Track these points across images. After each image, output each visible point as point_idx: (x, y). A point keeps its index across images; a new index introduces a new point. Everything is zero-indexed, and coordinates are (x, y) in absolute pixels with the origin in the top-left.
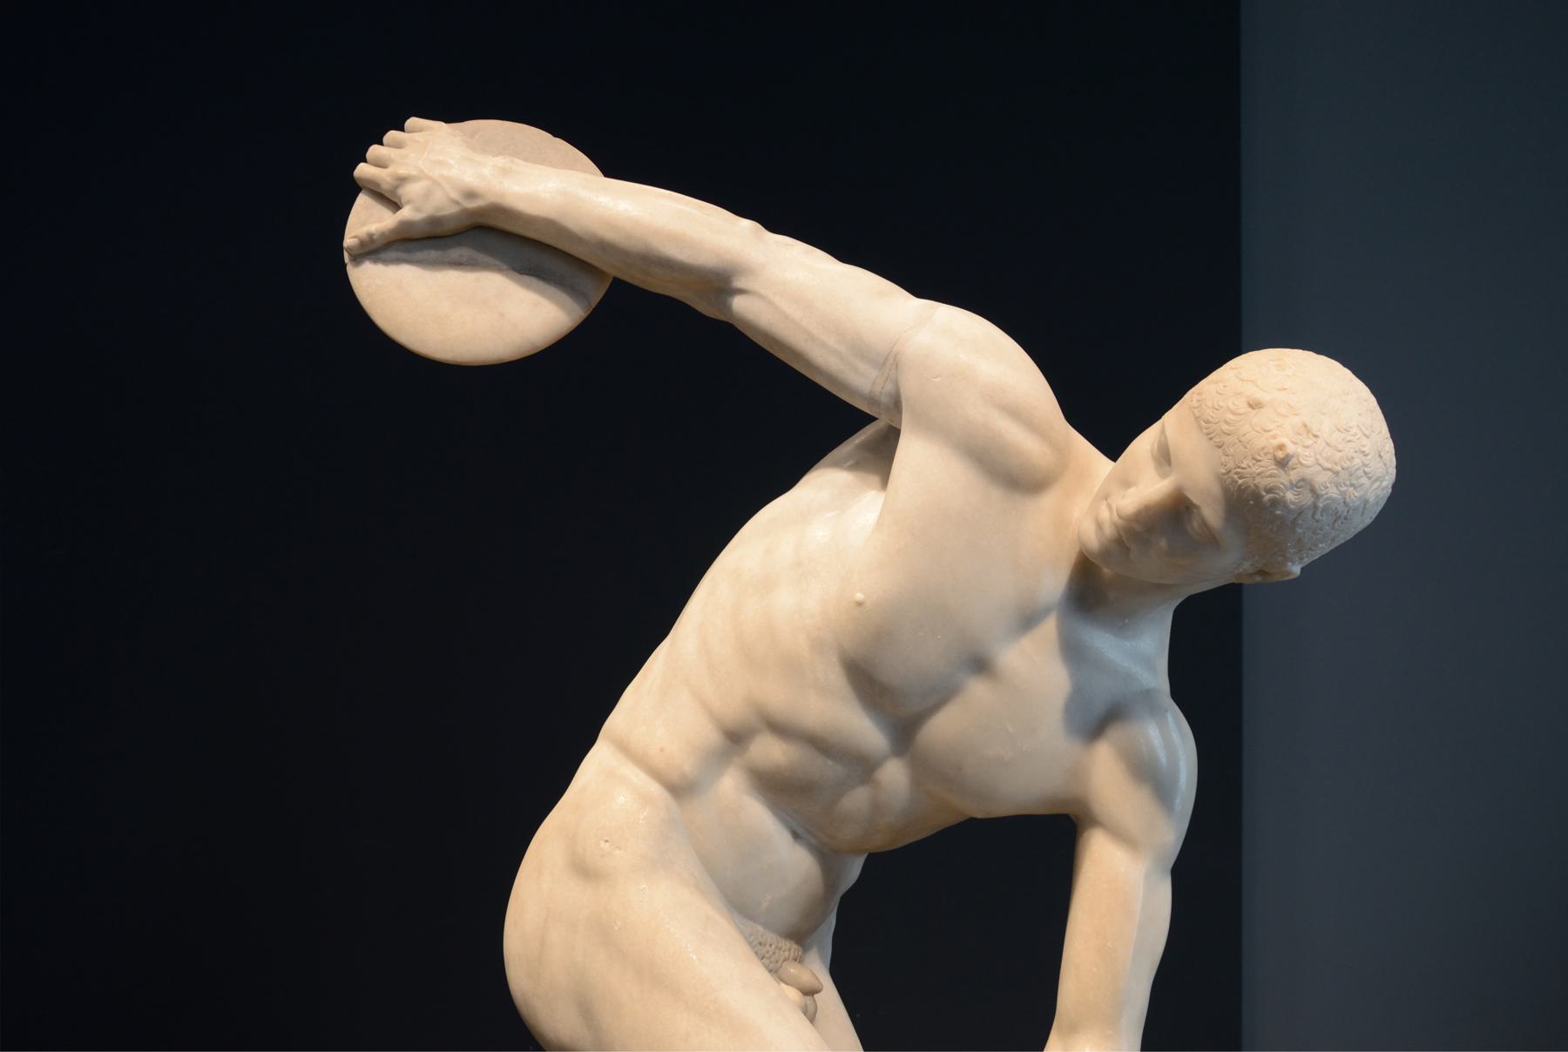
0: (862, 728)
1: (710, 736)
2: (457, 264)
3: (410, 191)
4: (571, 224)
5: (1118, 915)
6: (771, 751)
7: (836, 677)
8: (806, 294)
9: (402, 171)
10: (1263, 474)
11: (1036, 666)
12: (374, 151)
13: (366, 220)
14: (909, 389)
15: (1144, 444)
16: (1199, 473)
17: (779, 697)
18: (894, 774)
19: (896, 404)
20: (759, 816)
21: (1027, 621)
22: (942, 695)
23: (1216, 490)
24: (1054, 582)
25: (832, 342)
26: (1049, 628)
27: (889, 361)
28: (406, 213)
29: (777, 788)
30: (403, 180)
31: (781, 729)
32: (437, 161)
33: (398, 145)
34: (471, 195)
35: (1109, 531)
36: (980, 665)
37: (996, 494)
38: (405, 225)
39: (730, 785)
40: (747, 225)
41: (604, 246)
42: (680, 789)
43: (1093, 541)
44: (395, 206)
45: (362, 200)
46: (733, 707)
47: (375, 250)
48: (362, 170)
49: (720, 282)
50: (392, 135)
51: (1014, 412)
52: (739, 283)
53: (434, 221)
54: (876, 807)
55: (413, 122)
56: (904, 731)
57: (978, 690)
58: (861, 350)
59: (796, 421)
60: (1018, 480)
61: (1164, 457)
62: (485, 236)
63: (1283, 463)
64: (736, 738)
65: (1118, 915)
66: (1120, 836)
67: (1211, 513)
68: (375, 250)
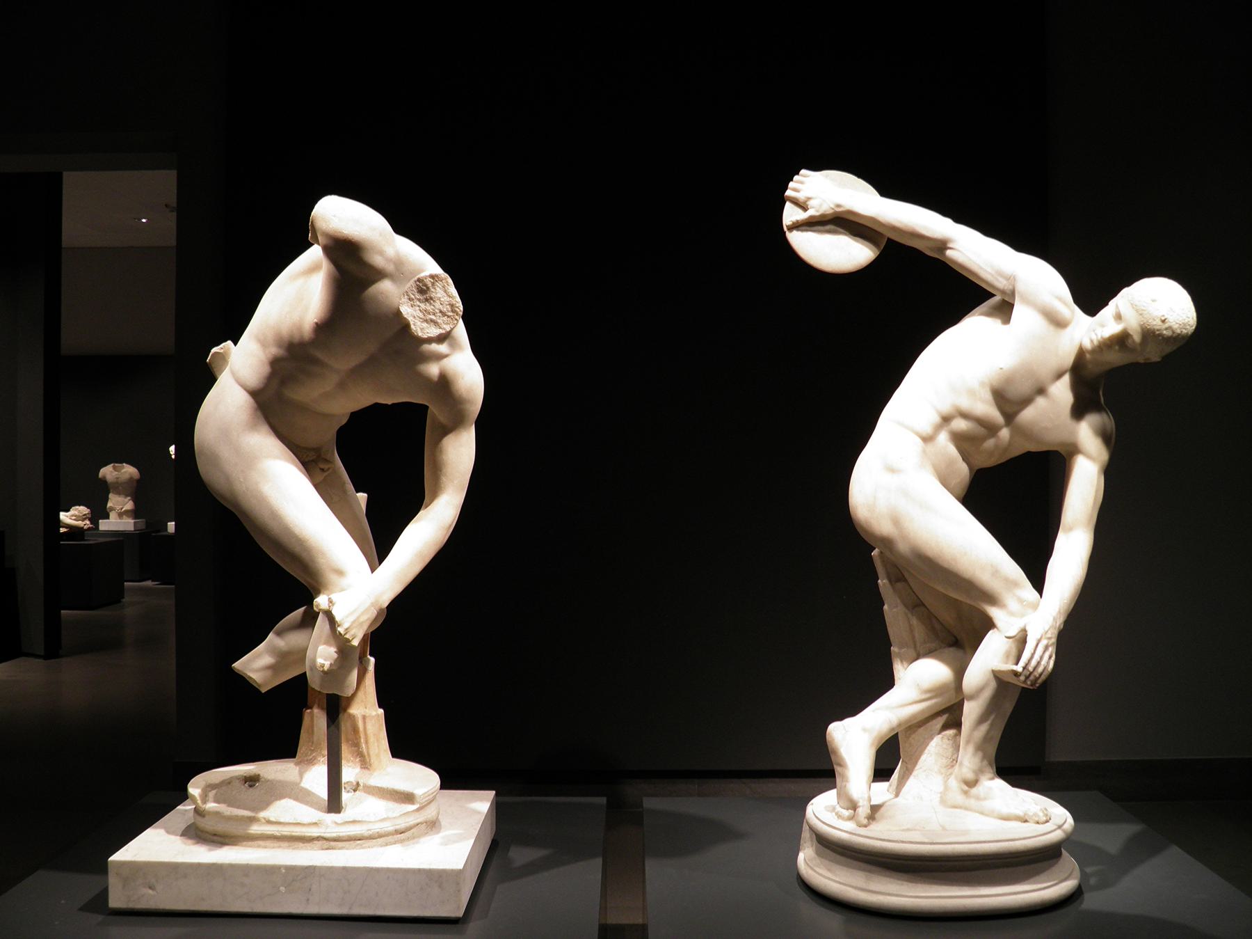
0: (994, 414)
1: (937, 419)
2: (829, 232)
3: (810, 203)
4: (880, 219)
5: (1084, 487)
6: (961, 425)
7: (988, 396)
8: (975, 250)
9: (809, 195)
10: (1156, 324)
11: (1062, 392)
12: (791, 184)
13: (791, 214)
14: (1020, 287)
15: (1107, 312)
16: (1132, 323)
17: (966, 404)
18: (1005, 433)
19: (1013, 293)
20: (952, 450)
21: (1059, 376)
22: (1026, 401)
23: (1139, 329)
24: (1069, 360)
25: (989, 270)
26: (1066, 379)
27: (1011, 278)
28: (811, 212)
29: (960, 440)
30: (809, 199)
31: (965, 415)
32: (820, 189)
33: (802, 183)
34: (838, 206)
35: (1096, 343)
36: (1041, 391)
37: (1052, 328)
38: (811, 217)
39: (943, 438)
40: (948, 221)
41: (894, 229)
42: (927, 439)
43: (1088, 345)
44: (805, 209)
45: (788, 205)
46: (946, 408)
47: (797, 226)
48: (788, 193)
49: (943, 245)
50: (796, 178)
51: (1060, 299)
52: (950, 245)
53: (823, 216)
54: (996, 446)
55: (803, 172)
56: (1009, 417)
57: (1040, 402)
58: (1001, 274)
59: (960, 295)
60: (1058, 323)
61: (1119, 317)
62: (844, 223)
63: (1163, 321)
64: (946, 419)
65: (1084, 487)
66: (1088, 456)
67: (1137, 338)
68: (797, 226)
